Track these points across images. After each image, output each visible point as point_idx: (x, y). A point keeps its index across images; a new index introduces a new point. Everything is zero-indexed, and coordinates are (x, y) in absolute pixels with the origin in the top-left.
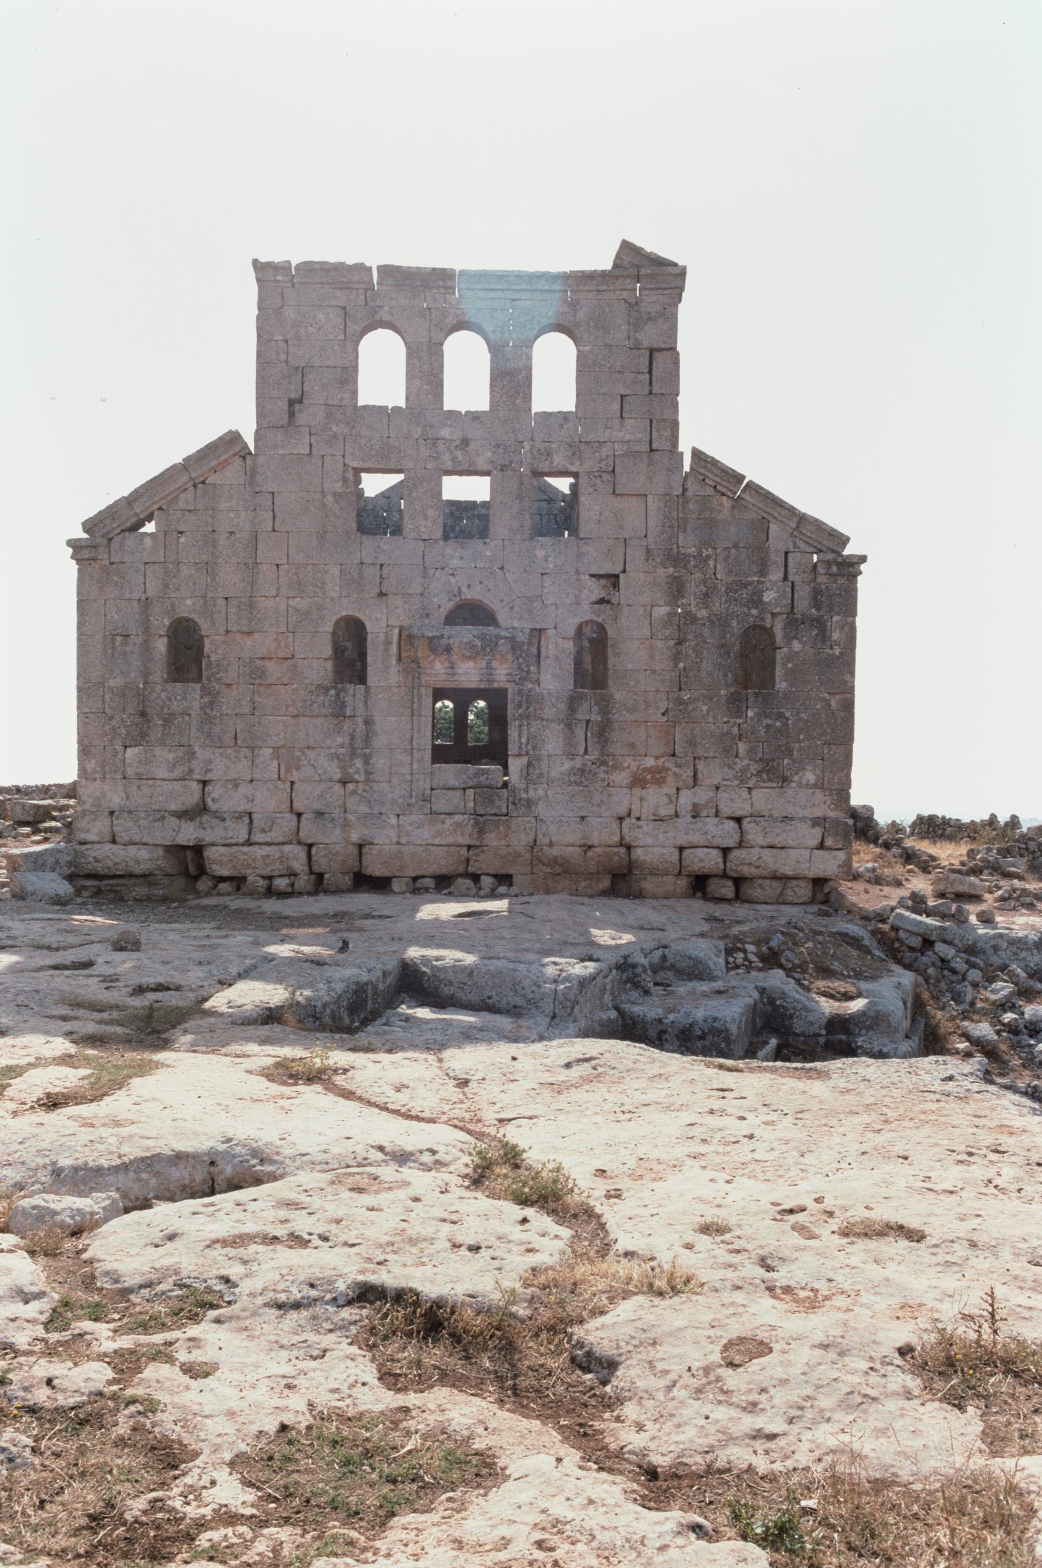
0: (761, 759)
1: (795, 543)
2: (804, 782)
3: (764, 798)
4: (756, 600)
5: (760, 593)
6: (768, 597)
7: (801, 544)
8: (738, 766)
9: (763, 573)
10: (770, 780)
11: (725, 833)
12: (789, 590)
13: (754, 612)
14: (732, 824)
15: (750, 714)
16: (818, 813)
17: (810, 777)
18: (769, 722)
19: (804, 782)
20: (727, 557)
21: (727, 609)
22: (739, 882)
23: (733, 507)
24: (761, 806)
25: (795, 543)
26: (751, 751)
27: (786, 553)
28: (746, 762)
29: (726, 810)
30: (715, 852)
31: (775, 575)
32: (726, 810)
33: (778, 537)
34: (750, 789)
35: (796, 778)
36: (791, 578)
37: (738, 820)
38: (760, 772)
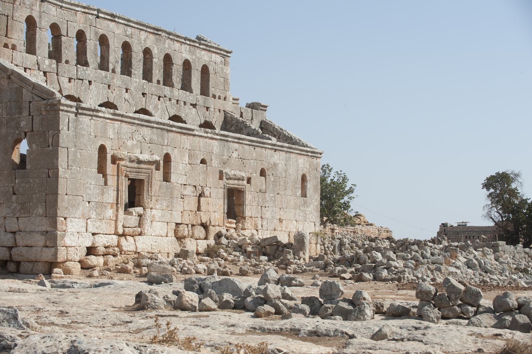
0: (21, 203)
1: (33, 97)
2: (38, 213)
3: (23, 223)
4: (18, 126)
5: (18, 123)
6: (23, 124)
7: (35, 97)
8: (13, 207)
9: (20, 113)
10: (24, 213)
11: (8, 239)
12: (31, 120)
13: (17, 132)
14: (11, 235)
15: (17, 181)
16: (44, 228)
17: (41, 211)
18: (24, 185)
19: (38, 213)
20: (7, 107)
21: (7, 132)
22: (18, 263)
23: (9, 83)
24: (22, 227)
25: (33, 97)
26: (18, 198)
27: (30, 102)
28: (15, 205)
29: (8, 229)
30: (4, 249)
31: (25, 113)
32: (8, 229)
33: (27, 95)
34: (18, 218)
35: (35, 212)
36: (31, 114)
37: (14, 233)
38: (20, 209)
